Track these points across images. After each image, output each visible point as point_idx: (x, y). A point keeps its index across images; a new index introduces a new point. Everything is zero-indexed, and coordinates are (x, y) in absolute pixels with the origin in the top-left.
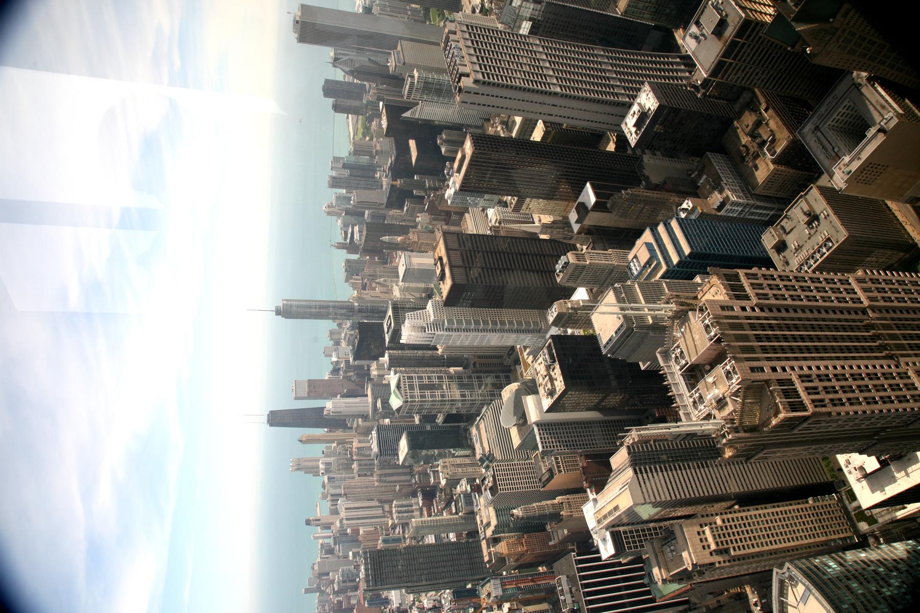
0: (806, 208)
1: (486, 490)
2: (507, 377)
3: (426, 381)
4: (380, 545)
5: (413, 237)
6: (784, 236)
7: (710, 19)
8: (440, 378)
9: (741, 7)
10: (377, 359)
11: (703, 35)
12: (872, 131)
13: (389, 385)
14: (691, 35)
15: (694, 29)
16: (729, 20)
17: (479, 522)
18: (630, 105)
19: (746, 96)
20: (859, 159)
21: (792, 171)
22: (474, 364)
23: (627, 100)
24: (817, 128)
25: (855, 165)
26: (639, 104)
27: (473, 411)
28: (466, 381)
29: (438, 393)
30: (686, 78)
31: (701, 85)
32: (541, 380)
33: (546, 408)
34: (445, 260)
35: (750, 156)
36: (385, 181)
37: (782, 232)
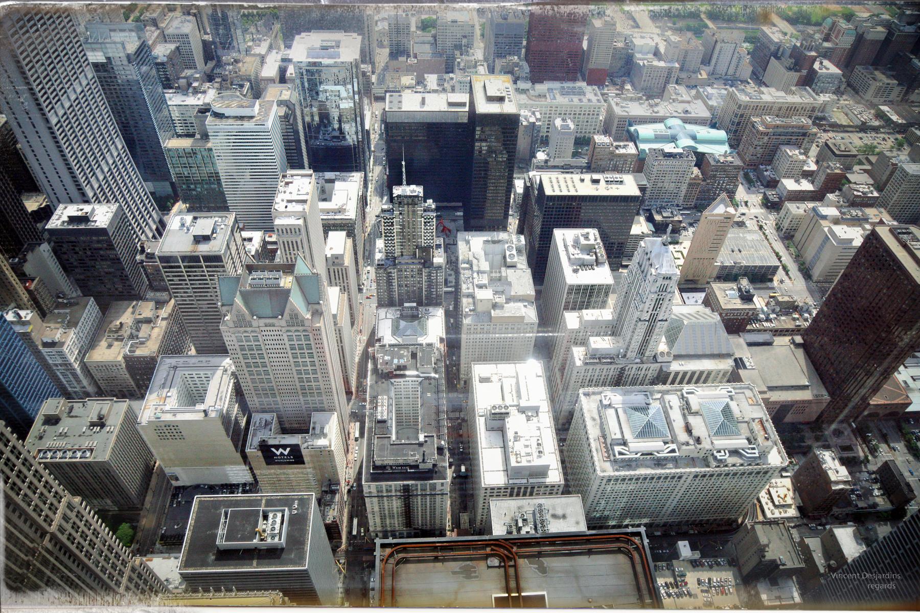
0: (104, 412)
6: (65, 415)
7: (204, 225)
9: (228, 245)
11: (188, 230)
12: (201, 407)
14: (182, 219)
15: (189, 218)
16: (212, 242)
18: (87, 202)
19: (164, 296)
20: (175, 415)
21: (128, 376)
23: (91, 194)
24: (175, 368)
25: (168, 417)
26: (93, 210)
30: (147, 236)
31: (148, 254)
35: (116, 335)
37: (67, 410)
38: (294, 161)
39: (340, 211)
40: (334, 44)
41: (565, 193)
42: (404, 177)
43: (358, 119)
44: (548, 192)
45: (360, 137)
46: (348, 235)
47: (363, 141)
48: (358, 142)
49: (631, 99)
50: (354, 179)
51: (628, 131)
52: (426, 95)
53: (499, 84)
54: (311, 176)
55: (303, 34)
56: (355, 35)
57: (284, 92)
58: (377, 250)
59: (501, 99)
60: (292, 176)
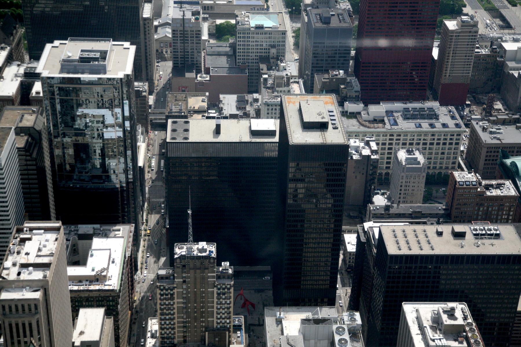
38: (35, 208)
39: (99, 278)
40: (98, 55)
41: (415, 251)
42: (190, 231)
43: (129, 153)
44: (392, 250)
45: (130, 176)
46: (108, 314)
47: (133, 183)
48: (128, 183)
49: (504, 122)
50: (120, 233)
51: (503, 165)
52: (224, 123)
53: (320, 106)
54: (58, 229)
55: (57, 43)
56: (127, 44)
57: (26, 116)
58: (149, 335)
59: (322, 126)
60: (31, 229)
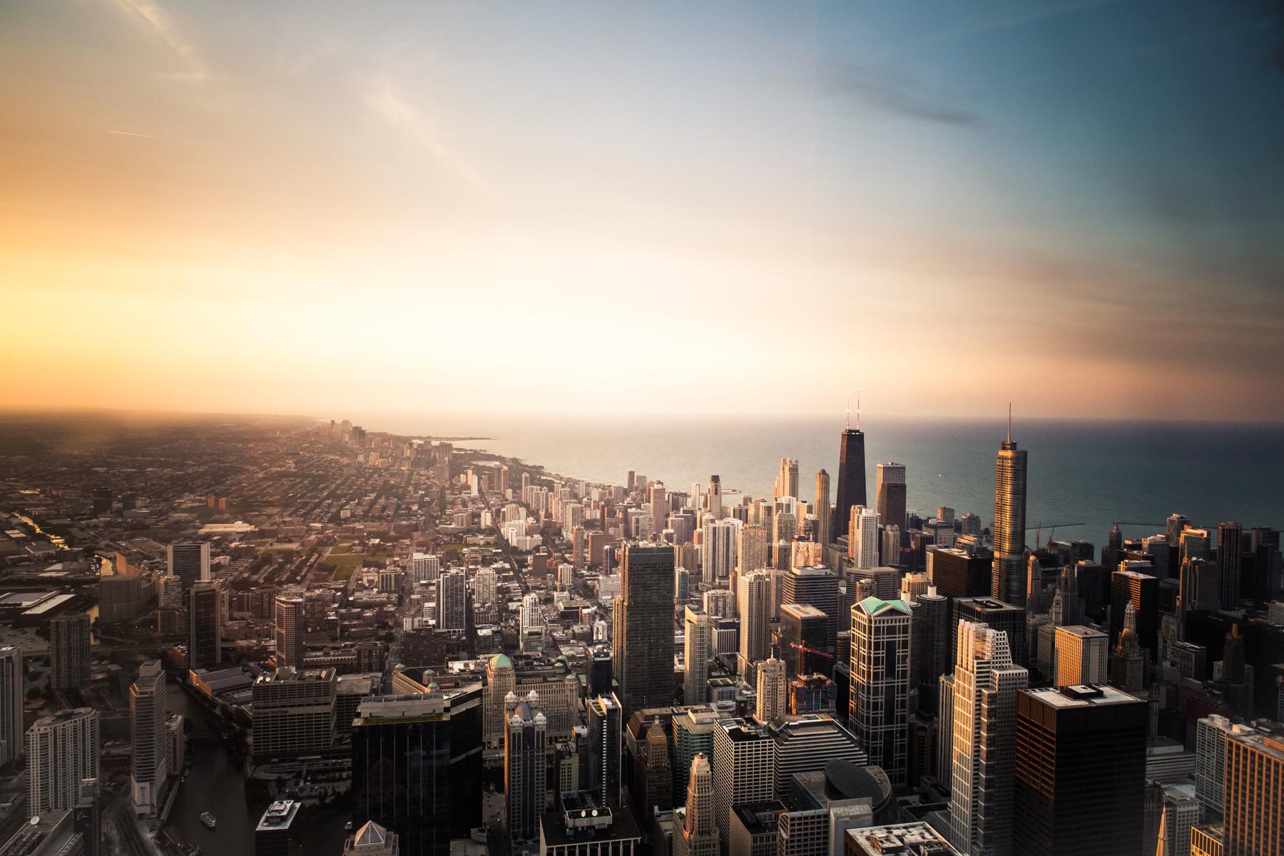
1: (738, 722)
2: (901, 779)
3: (899, 652)
4: (679, 570)
5: (1136, 654)
8: (904, 672)
10: (935, 584)
13: (896, 597)
17: (696, 707)
22: (923, 729)
27: (851, 718)
28: (898, 712)
29: (882, 669)
32: (896, 832)
33: (852, 832)
34: (1098, 701)
36: (1240, 613)
